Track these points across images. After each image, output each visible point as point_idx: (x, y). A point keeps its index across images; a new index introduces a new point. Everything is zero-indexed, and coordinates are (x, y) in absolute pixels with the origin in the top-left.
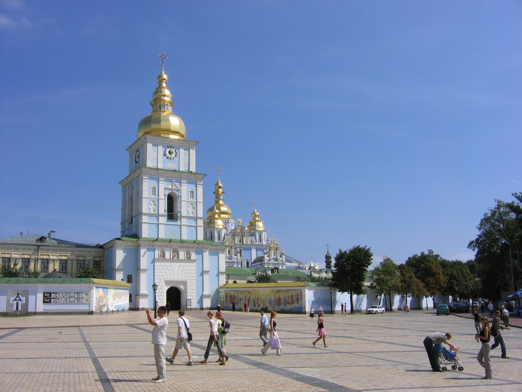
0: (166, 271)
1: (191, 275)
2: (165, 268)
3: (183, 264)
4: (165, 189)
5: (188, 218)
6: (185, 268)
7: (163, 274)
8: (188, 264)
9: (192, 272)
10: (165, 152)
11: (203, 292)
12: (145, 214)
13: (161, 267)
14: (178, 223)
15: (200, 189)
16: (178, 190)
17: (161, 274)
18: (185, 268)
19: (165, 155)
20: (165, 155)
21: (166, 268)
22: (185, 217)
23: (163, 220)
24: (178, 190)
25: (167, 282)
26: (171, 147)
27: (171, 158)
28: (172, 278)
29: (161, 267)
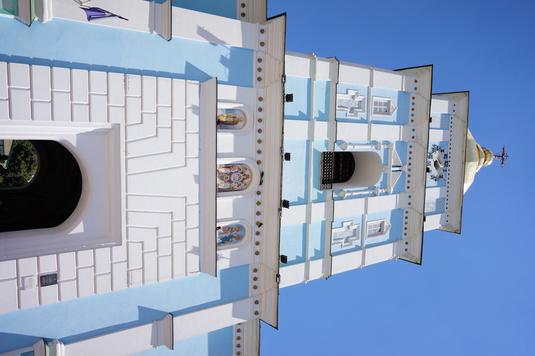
0: (165, 134)
1: (151, 259)
2: (179, 128)
5: (328, 224)
6: (179, 228)
7: (150, 120)
9: (165, 263)
11: (66, 341)
12: (335, 75)
14: (314, 193)
15: (385, 253)
16: (384, 185)
17: (150, 107)
18: (179, 228)
24: (384, 185)
25: (109, 138)
28: (134, 166)
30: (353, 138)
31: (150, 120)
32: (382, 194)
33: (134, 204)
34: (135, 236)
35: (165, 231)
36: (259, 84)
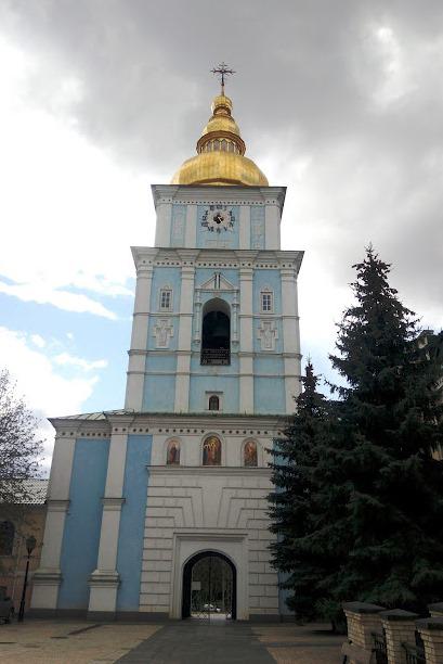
2: (177, 492)
3: (235, 481)
4: (196, 291)
6: (242, 494)
7: (172, 512)
8: (251, 481)
10: (205, 218)
13: (168, 492)
17: (163, 512)
19: (205, 224)
20: (205, 224)
21: (181, 492)
22: (246, 355)
23: (184, 363)
26: (219, 207)
27: (218, 230)
29: (168, 492)
30: (189, 332)
31: (172, 512)
32: (238, 299)
33: (222, 524)
34: (242, 525)
35: (241, 503)
36: (151, 431)
